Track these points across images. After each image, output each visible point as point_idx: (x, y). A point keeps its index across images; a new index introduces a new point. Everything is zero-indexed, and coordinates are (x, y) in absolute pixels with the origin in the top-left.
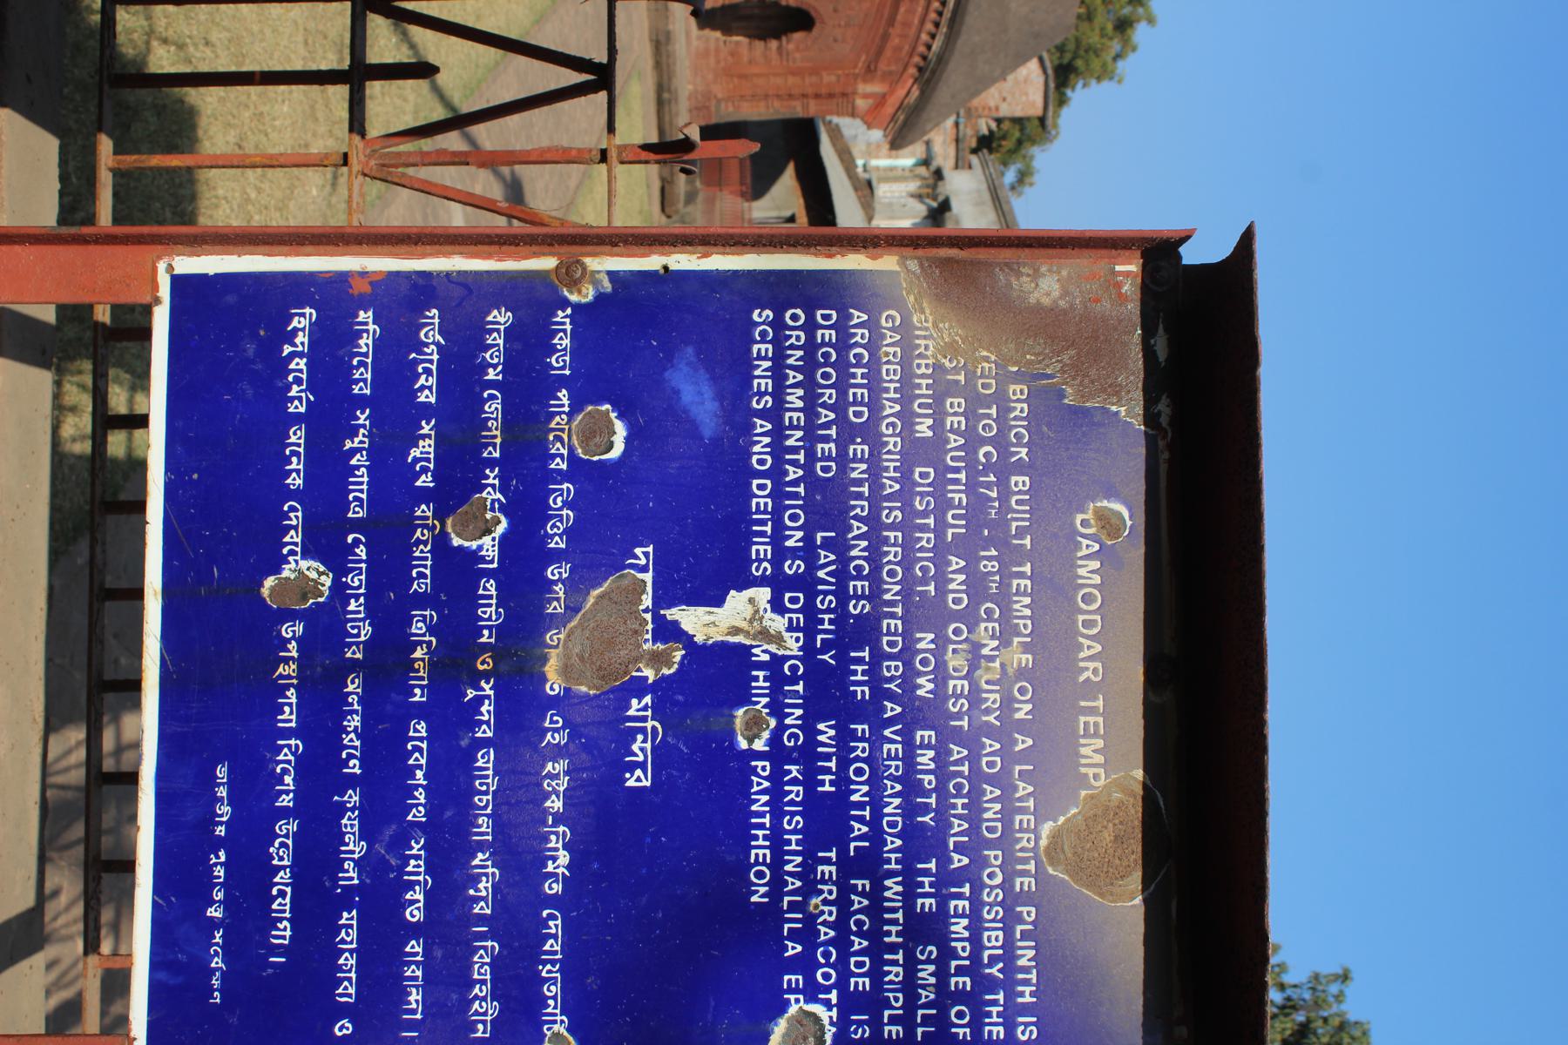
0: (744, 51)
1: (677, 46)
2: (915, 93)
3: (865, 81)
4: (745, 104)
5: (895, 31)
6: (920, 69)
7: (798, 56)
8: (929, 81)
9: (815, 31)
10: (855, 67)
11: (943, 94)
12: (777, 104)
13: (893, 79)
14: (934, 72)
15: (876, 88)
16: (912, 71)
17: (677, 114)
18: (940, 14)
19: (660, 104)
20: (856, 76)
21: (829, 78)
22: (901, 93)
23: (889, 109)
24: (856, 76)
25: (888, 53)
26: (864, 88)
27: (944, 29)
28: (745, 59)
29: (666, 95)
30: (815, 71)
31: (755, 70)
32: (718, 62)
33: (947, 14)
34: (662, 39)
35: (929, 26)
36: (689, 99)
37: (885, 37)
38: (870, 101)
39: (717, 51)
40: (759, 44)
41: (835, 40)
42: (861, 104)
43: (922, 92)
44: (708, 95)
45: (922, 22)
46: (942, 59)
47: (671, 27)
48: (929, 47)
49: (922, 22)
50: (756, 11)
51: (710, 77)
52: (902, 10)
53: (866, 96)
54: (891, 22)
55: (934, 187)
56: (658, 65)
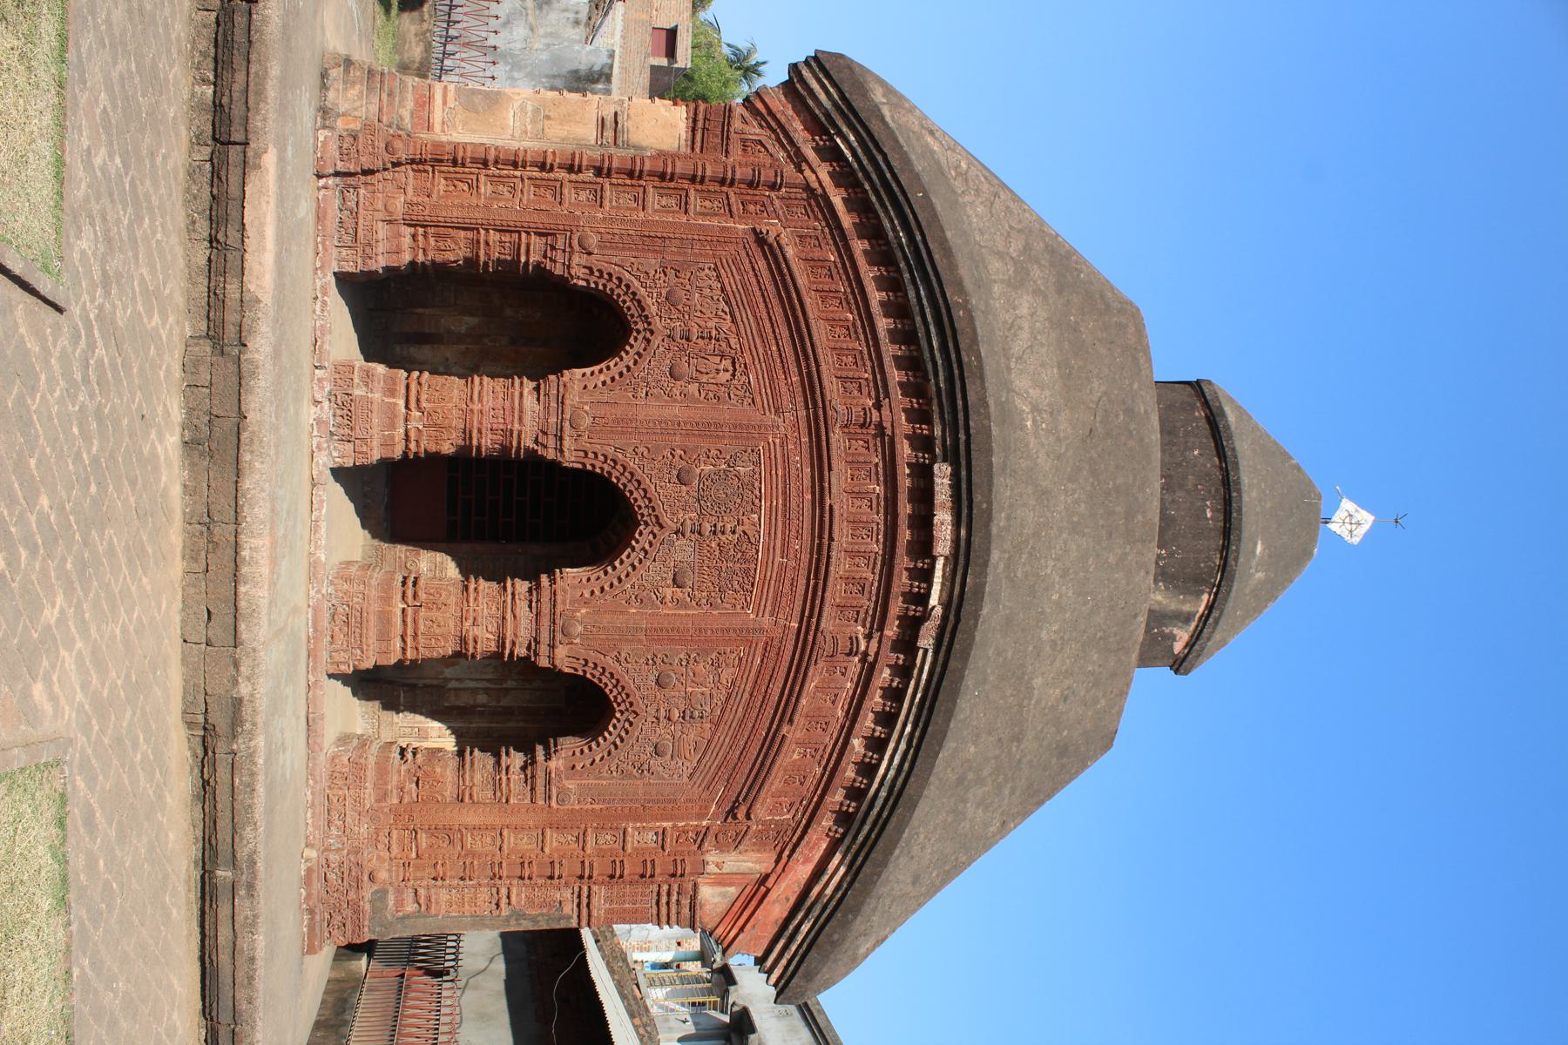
0: (448, 771)
1: (260, 741)
2: (837, 868)
3: (720, 847)
4: (444, 895)
5: (793, 733)
6: (844, 818)
7: (571, 785)
8: (870, 845)
9: (613, 732)
10: (701, 816)
11: (899, 872)
12: (519, 895)
13: (787, 845)
14: (881, 825)
15: (749, 862)
16: (826, 821)
17: (252, 925)
18: (894, 695)
19: (207, 892)
20: (701, 837)
21: (641, 837)
22: (801, 871)
23: (776, 908)
24: (701, 837)
25: (775, 782)
26: (712, 857)
27: (905, 726)
28: (449, 792)
29: (223, 873)
30: (610, 820)
31: (470, 817)
32: (383, 796)
33: (913, 693)
34: (220, 719)
35: (867, 722)
36: (308, 880)
37: (772, 744)
38: (733, 891)
39: (382, 770)
40: (482, 760)
41: (658, 752)
42: (714, 898)
43: (854, 872)
44: (356, 875)
45: (853, 714)
46: (897, 795)
47: (244, 689)
48: (867, 770)
49: (853, 714)
50: (482, 698)
51: (364, 829)
52: (811, 685)
53: (722, 880)
54: (786, 710)
55: (724, 994)
56: (206, 790)
